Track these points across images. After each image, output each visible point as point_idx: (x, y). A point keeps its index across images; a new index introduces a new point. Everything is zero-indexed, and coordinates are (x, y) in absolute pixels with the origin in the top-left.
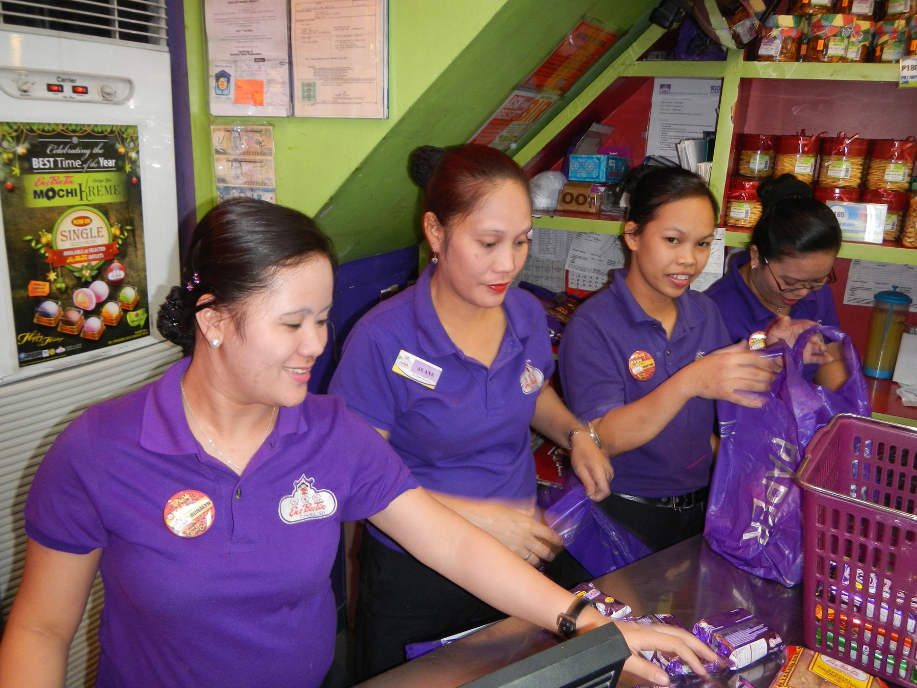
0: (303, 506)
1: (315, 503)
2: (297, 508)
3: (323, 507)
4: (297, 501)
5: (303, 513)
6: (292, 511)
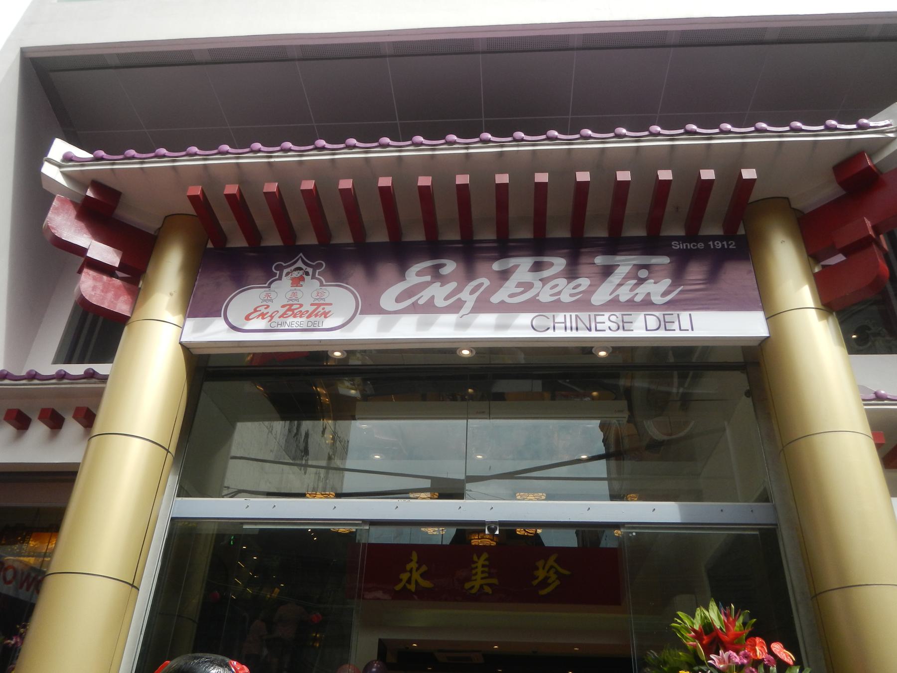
0: (283, 306)
1: (312, 305)
2: (268, 307)
3: (326, 315)
4: (273, 295)
5: (276, 319)
6: (255, 310)
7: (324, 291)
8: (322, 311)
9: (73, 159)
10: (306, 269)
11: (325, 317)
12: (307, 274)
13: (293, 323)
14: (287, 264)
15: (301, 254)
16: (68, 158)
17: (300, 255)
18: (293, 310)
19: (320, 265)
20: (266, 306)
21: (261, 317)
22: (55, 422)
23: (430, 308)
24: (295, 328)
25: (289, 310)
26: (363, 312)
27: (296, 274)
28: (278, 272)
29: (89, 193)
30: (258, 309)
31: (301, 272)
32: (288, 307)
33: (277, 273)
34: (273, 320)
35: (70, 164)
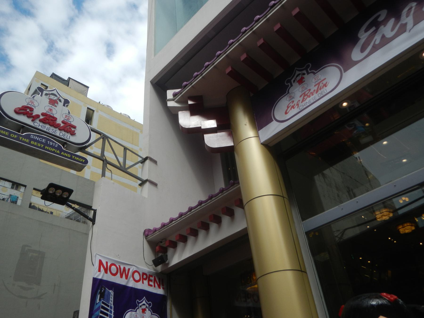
0: (301, 97)
1: (315, 86)
2: (293, 101)
3: (325, 85)
5: (300, 104)
6: (288, 107)
7: (318, 75)
8: (322, 85)
9: (177, 93)
10: (302, 72)
11: (326, 86)
12: (304, 74)
13: (310, 101)
14: (291, 78)
15: (296, 68)
16: (175, 95)
17: (295, 69)
18: (307, 95)
19: (308, 66)
20: (292, 102)
21: (292, 108)
22: (231, 214)
23: (385, 41)
24: (313, 102)
25: (305, 96)
26: (345, 70)
27: (298, 78)
28: (289, 84)
29: (190, 102)
30: (289, 106)
31: (300, 76)
32: (303, 95)
33: (289, 85)
34: (299, 106)
35: (177, 96)
